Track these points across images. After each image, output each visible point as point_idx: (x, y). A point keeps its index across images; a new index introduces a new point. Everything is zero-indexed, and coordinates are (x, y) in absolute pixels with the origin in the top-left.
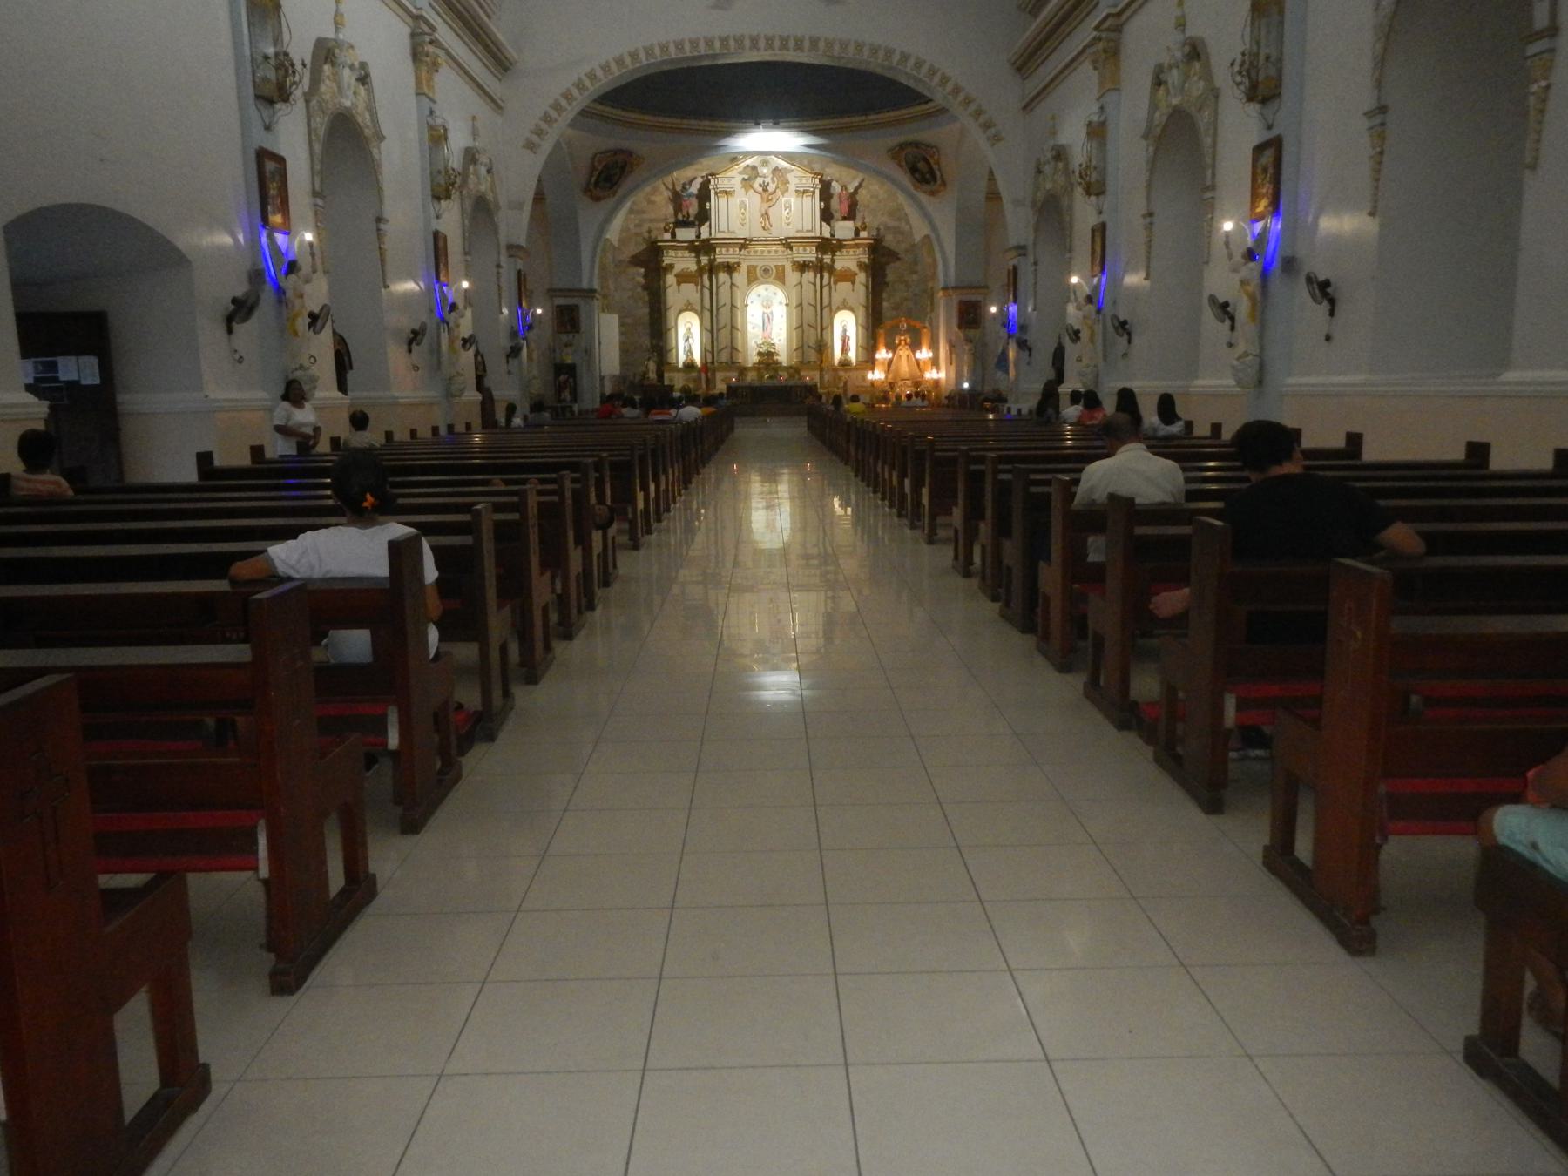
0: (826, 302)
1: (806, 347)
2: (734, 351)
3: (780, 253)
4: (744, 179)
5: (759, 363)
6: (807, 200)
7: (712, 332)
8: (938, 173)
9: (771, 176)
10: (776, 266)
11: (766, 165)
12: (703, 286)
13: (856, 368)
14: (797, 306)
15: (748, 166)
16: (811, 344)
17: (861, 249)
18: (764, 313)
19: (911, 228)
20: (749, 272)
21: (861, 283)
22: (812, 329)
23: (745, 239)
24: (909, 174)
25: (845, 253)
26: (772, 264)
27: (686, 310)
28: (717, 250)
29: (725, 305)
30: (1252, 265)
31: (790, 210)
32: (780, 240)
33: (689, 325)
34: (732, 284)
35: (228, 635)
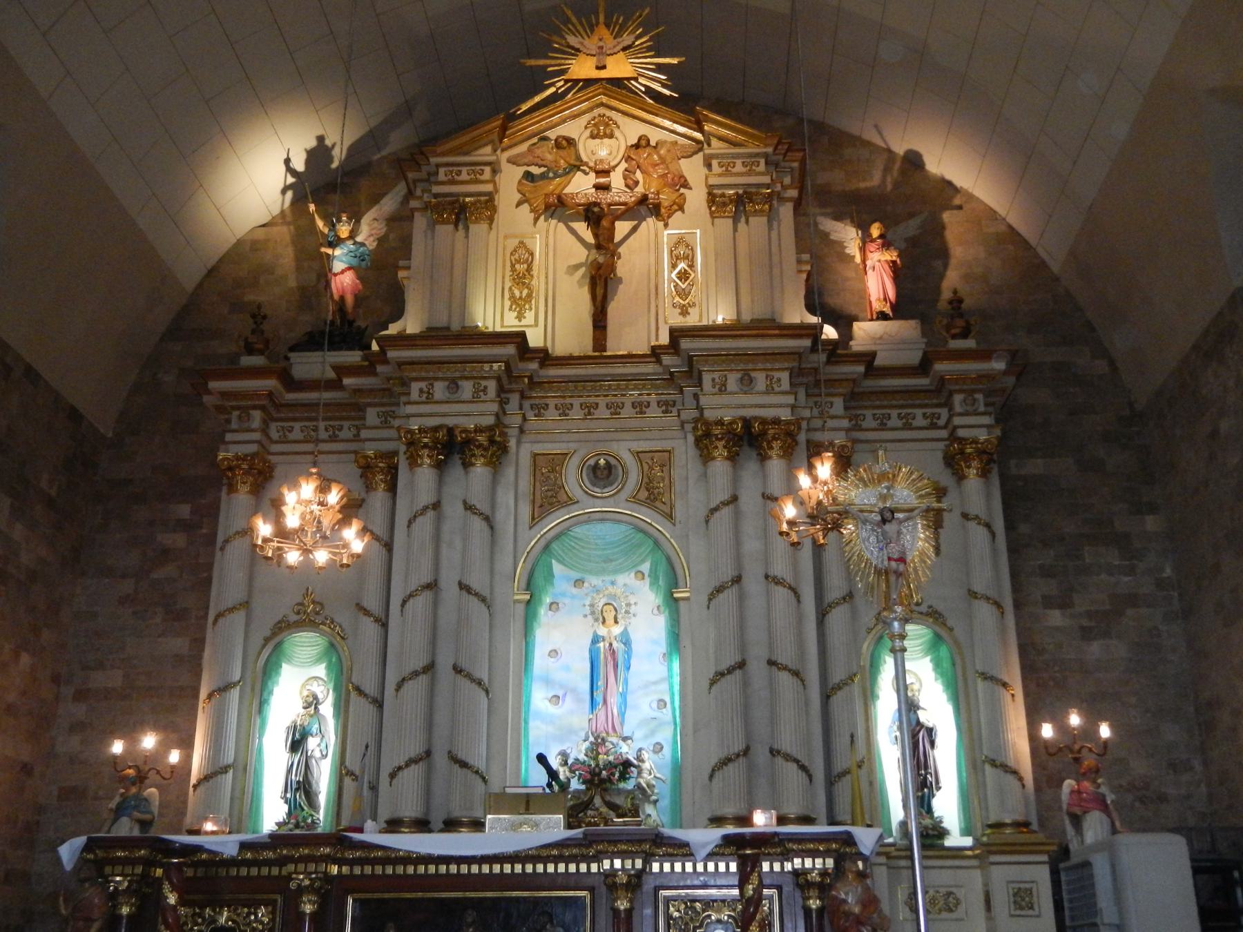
1: (761, 755)
3: (654, 412)
4: (528, 176)
7: (379, 703)
9: (624, 165)
10: (638, 455)
11: (611, 136)
15: (546, 139)
16: (787, 743)
17: (958, 398)
18: (596, 640)
19: (1112, 363)
21: (965, 516)
22: (784, 677)
23: (519, 338)
25: (894, 422)
26: (624, 450)
27: (299, 625)
28: (415, 387)
31: (691, 266)
32: (656, 353)
33: (318, 689)
34: (468, 507)
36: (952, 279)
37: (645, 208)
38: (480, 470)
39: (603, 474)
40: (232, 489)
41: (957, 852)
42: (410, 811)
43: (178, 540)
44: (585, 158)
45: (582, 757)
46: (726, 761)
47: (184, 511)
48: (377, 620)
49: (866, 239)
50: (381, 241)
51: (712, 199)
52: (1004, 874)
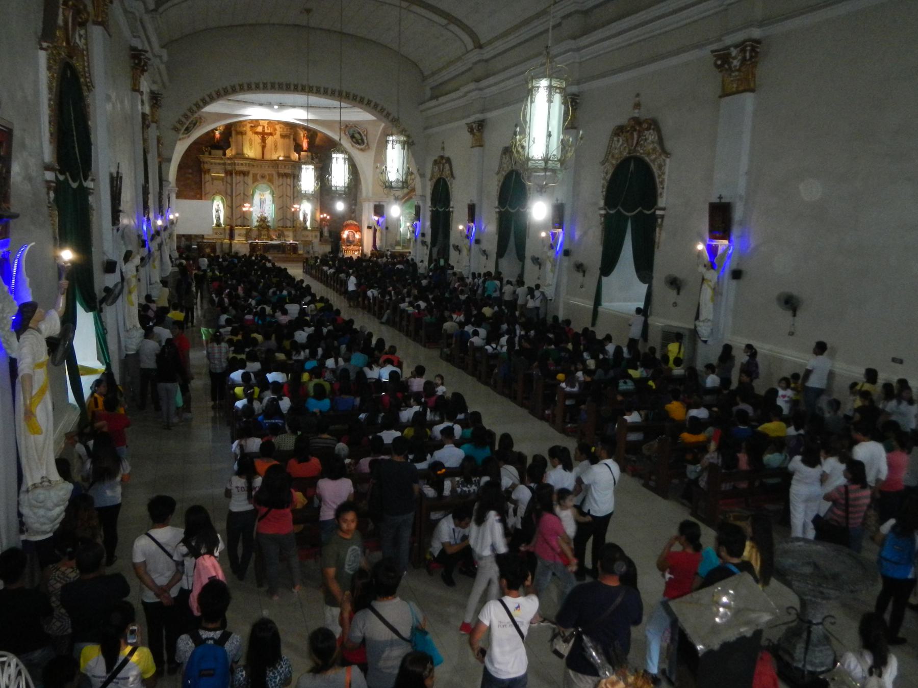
0: (295, 195)
2: (246, 220)
3: (271, 167)
4: (251, 126)
5: (260, 226)
6: (287, 140)
8: (365, 141)
10: (269, 175)
12: (227, 182)
13: (311, 231)
14: (280, 197)
18: (261, 199)
20: (253, 177)
24: (350, 140)
26: (266, 173)
29: (240, 194)
30: (552, 251)
33: (218, 203)
34: (244, 183)
35: (653, 477)
36: (318, 139)
37: (271, 134)
38: (246, 178)
39: (263, 177)
40: (205, 174)
41: (309, 230)
42: (239, 224)
43: (190, 176)
44: (261, 124)
45: (259, 216)
46: (280, 220)
47: (190, 171)
48: (230, 196)
49: (304, 136)
50: (224, 130)
51: (281, 135)
52: (314, 234)
